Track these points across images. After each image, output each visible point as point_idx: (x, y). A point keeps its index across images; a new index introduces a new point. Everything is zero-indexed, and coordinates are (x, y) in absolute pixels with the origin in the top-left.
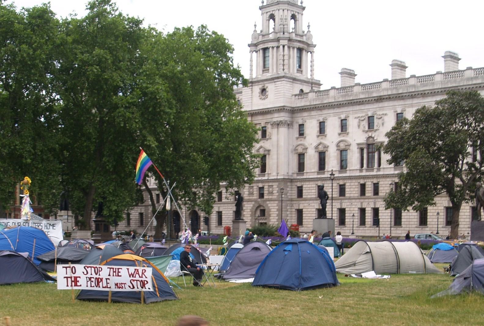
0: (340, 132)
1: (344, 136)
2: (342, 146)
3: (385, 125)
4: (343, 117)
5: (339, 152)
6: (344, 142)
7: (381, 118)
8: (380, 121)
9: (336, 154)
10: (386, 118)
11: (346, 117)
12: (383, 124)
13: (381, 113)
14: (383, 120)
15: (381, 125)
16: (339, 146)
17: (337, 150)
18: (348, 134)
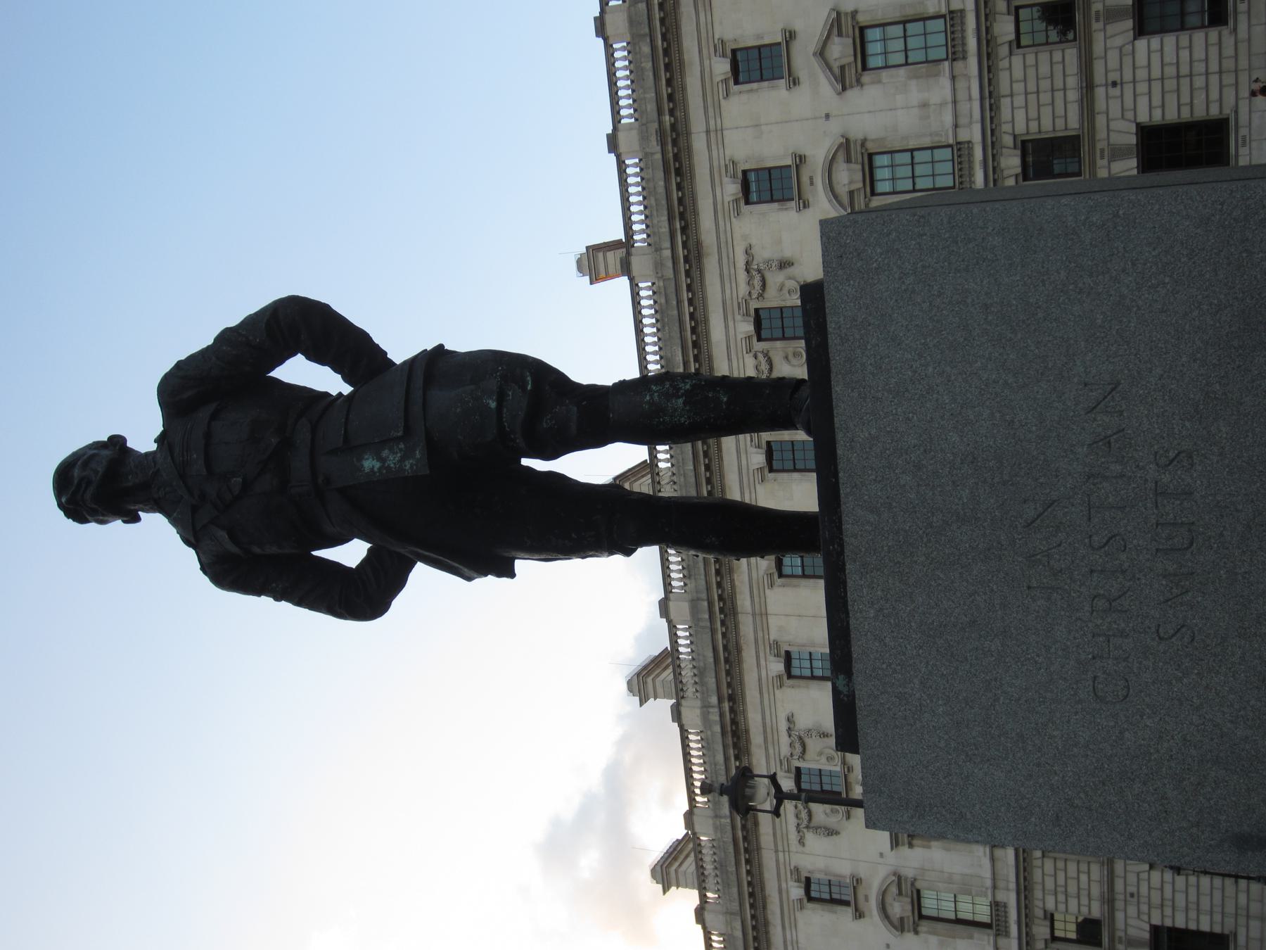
0: (849, 911)
1: (867, 898)
2: (899, 908)
3: (787, 254)
4: (797, 892)
5: (924, 926)
6: (889, 899)
7: (759, 271)
8: (775, 278)
9: (934, 940)
10: (764, 253)
11: (798, 881)
12: (784, 264)
13: (742, 276)
14: (768, 262)
15: (789, 271)
16: (902, 919)
17: (916, 933)
18: (859, 881)
